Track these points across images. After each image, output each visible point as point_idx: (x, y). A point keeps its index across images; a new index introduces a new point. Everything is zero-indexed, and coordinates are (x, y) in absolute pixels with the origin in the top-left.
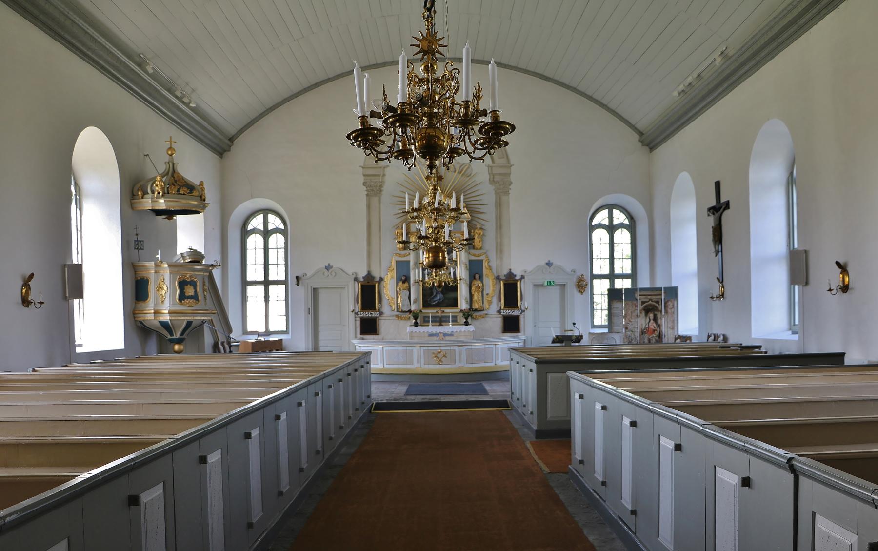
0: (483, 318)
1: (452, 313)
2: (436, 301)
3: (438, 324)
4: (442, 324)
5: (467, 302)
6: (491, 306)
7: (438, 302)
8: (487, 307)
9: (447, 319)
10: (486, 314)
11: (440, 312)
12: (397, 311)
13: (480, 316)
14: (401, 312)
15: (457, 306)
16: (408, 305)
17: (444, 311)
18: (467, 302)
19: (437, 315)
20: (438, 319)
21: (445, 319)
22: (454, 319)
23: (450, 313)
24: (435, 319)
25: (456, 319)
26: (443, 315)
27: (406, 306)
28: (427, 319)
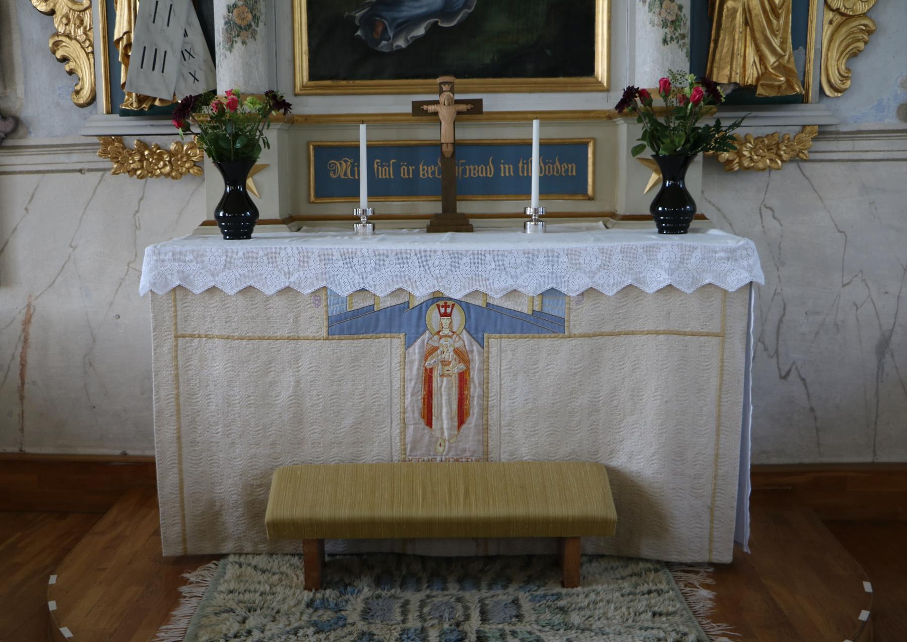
0: (796, 159)
1: (546, 117)
2: (415, 21)
3: (433, 207)
4: (463, 207)
5: (675, 23)
6: (861, 66)
7: (434, 29)
8: (835, 67)
9: (506, 170)
10: (823, 133)
11: (445, 113)
12: (111, 111)
13: (772, 145)
14: (139, 114)
15: (588, 68)
16: (186, 54)
17: (476, 107)
18: (675, 23)
19: (425, 133)
20: (427, 171)
21: (476, 171)
22: (559, 168)
23: (525, 117)
24: (406, 172)
25: (573, 170)
26: (471, 133)
27: (173, 62)
28: (341, 168)
